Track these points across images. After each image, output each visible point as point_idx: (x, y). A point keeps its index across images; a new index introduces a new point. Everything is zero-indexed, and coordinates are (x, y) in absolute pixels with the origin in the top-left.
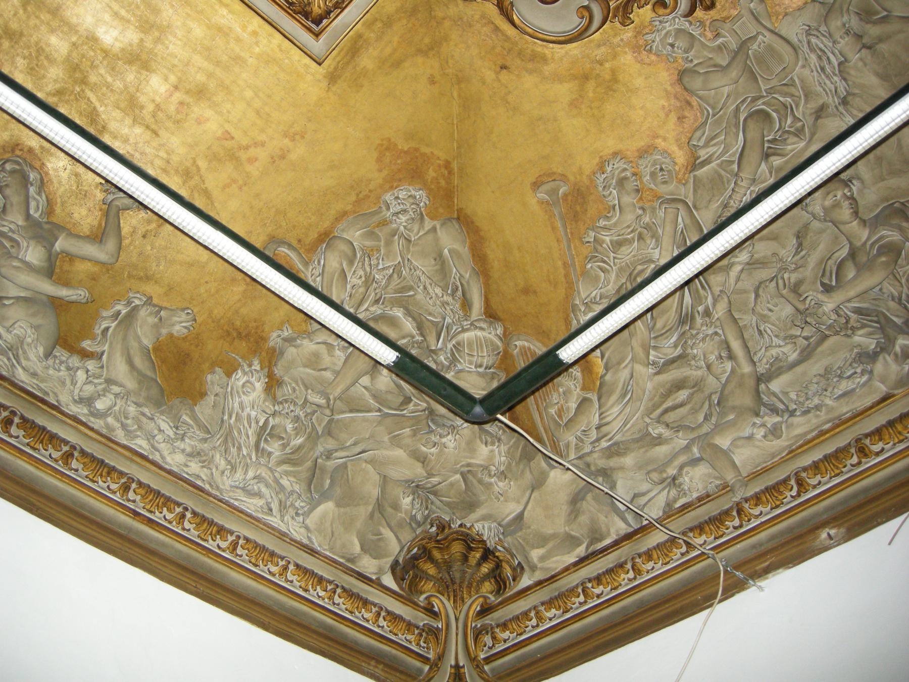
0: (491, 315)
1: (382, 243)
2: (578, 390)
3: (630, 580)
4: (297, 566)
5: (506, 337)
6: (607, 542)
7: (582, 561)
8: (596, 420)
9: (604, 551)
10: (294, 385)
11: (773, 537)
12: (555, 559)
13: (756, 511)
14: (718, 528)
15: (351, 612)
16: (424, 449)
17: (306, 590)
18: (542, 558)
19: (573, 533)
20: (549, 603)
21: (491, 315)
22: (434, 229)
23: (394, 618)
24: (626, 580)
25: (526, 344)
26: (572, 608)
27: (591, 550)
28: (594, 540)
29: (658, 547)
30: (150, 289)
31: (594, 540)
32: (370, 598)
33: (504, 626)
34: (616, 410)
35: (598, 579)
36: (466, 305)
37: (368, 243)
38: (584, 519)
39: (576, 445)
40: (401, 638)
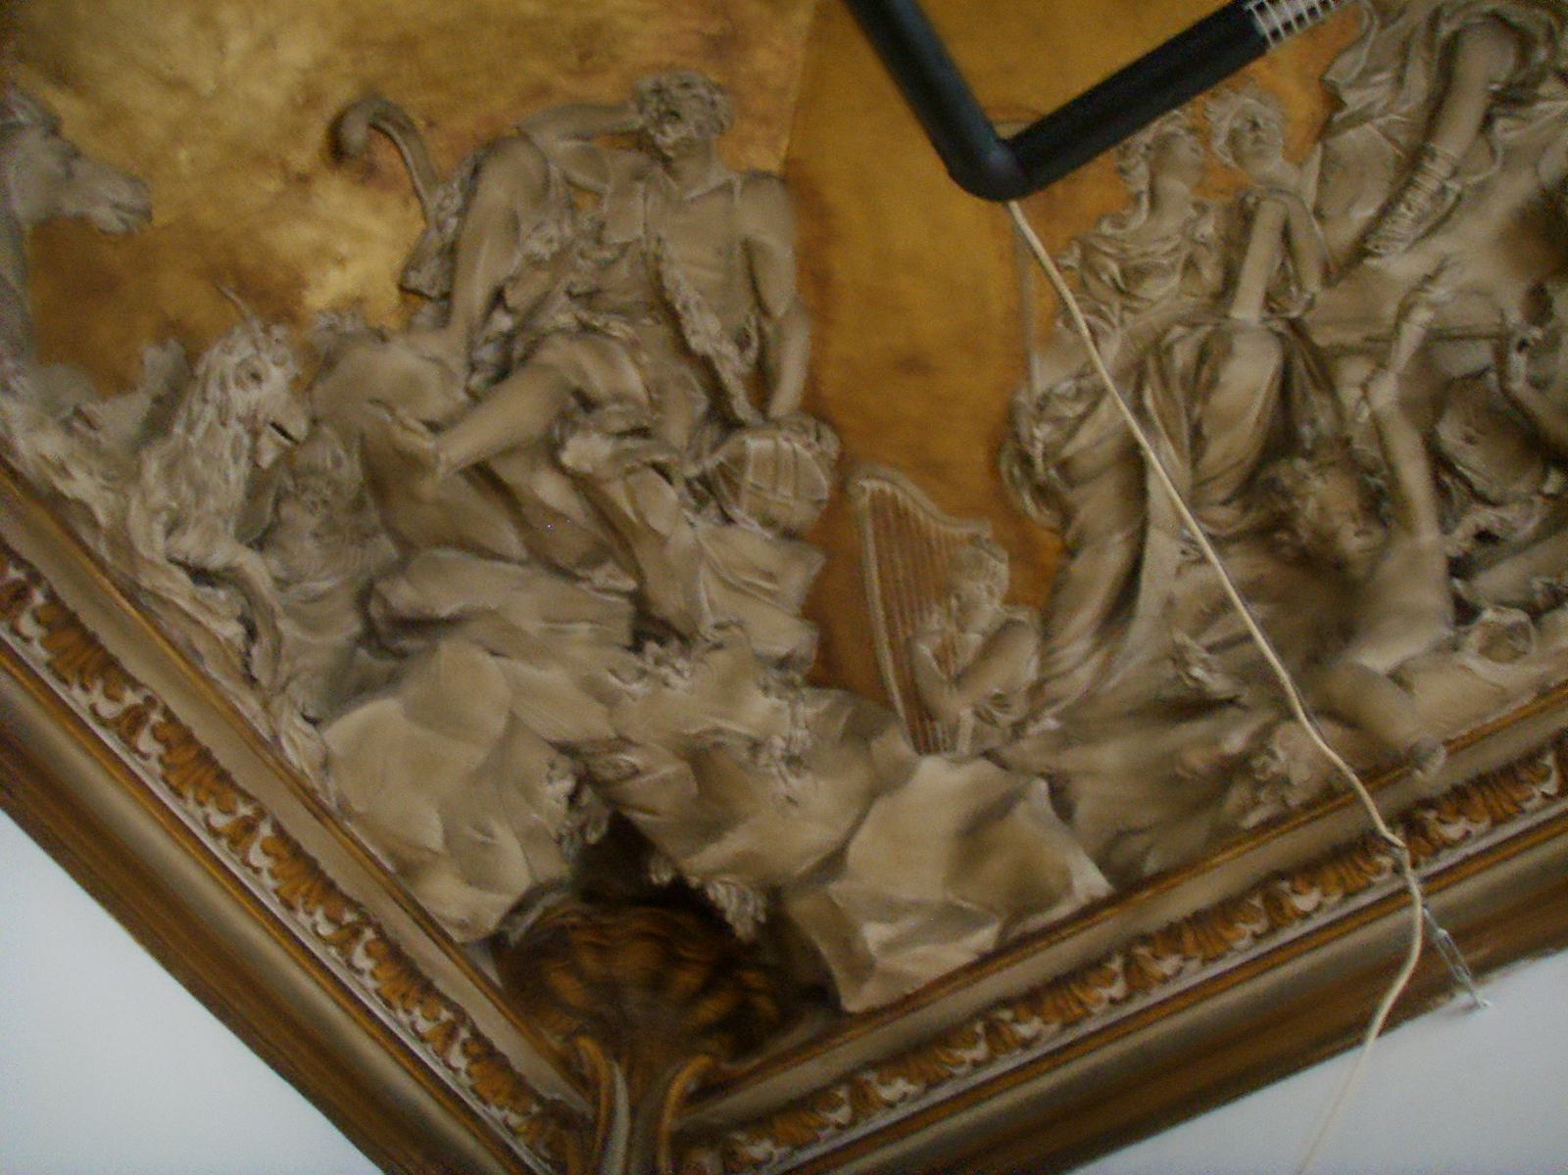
0: (815, 408)
1: (609, 188)
2: (997, 604)
3: (1113, 1001)
4: (279, 830)
5: (843, 468)
6: (1062, 910)
7: (985, 962)
8: (1030, 671)
9: (1051, 933)
10: (341, 453)
11: (1493, 893)
12: (921, 950)
13: (1453, 831)
14: (1359, 869)
15: (388, 1003)
16: (614, 680)
17: (289, 906)
18: (889, 947)
19: (965, 905)
20: (895, 1061)
21: (815, 408)
22: (727, 189)
23: (484, 1052)
24: (1104, 1006)
25: (888, 488)
26: (951, 1076)
27: (1017, 931)
28: (1018, 914)
29: (1197, 919)
30: (62, 103)
31: (1018, 914)
32: (440, 985)
33: (759, 1122)
34: (1080, 647)
35: (1031, 1000)
36: (763, 381)
37: (579, 177)
38: (997, 868)
39: (975, 730)
40: (493, 1114)
